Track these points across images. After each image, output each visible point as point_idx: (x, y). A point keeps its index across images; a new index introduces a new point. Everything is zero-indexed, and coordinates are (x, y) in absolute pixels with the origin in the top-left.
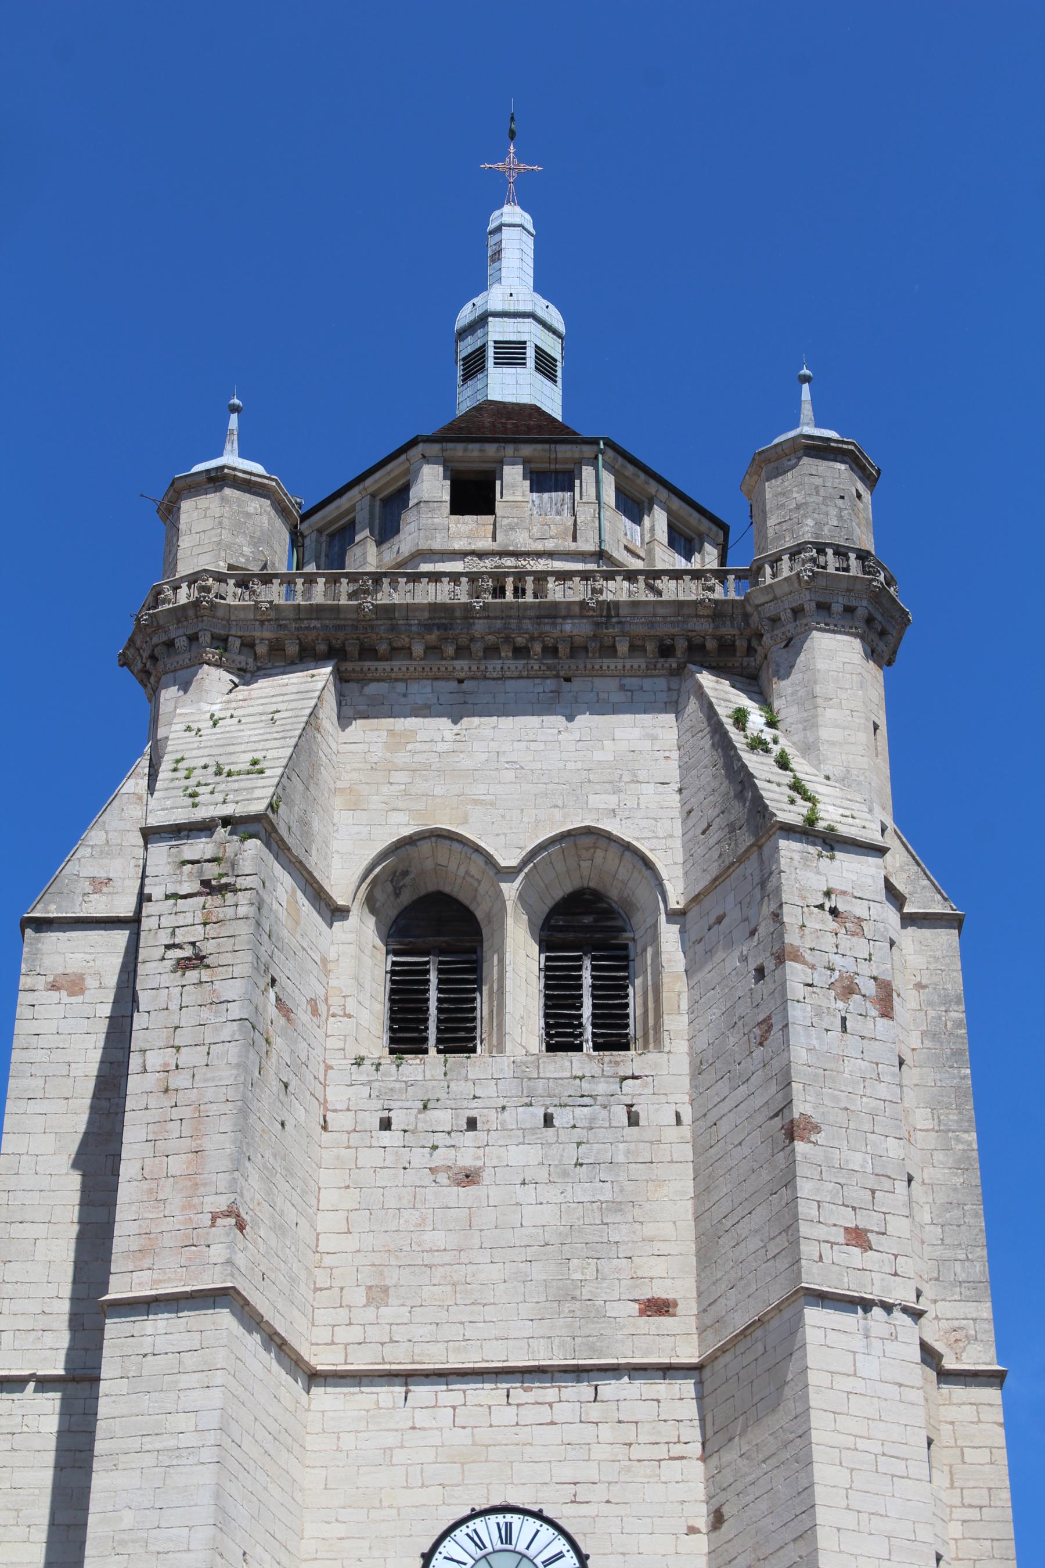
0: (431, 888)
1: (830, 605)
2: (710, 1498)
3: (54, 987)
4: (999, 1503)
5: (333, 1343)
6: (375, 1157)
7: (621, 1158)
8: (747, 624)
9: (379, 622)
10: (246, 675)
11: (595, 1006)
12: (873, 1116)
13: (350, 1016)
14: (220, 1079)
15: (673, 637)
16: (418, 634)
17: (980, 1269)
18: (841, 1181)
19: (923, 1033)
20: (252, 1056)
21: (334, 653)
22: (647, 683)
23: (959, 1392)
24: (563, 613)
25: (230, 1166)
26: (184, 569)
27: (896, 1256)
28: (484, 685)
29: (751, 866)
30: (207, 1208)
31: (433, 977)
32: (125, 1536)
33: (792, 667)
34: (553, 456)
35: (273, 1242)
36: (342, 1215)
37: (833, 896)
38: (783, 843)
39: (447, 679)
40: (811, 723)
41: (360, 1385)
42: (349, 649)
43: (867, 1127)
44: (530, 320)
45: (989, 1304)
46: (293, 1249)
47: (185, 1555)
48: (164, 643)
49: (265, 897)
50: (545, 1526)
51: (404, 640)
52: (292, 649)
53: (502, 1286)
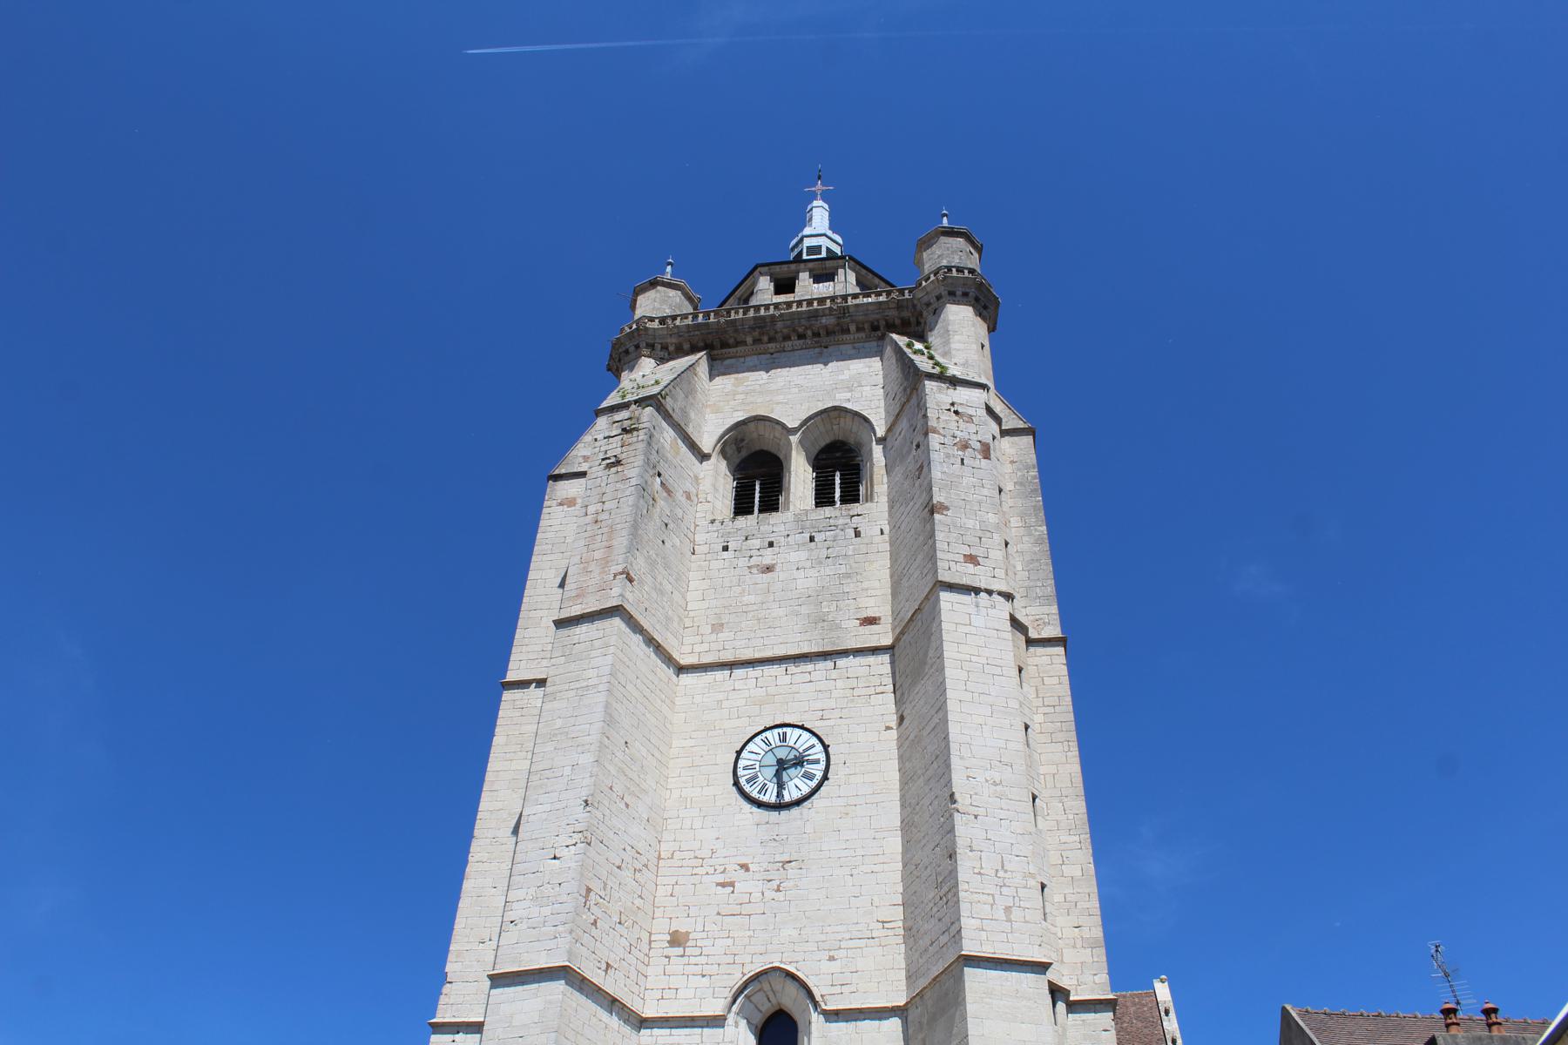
0: (758, 448)
2: (897, 711)
3: (561, 504)
5: (692, 652)
6: (720, 564)
7: (850, 553)
10: (662, 360)
11: (841, 492)
12: (980, 503)
13: (709, 502)
15: (878, 321)
16: (749, 332)
17: (1050, 589)
18: (962, 533)
19: (1015, 483)
20: (641, 501)
21: (708, 347)
22: (867, 345)
23: (1040, 650)
24: (821, 314)
26: (636, 317)
27: (994, 568)
28: (784, 354)
29: (914, 401)
32: (557, 732)
33: (937, 322)
35: (654, 595)
38: (926, 382)
39: (764, 354)
40: (947, 342)
42: (715, 343)
43: (976, 508)
44: (824, 237)
45: (1056, 606)
48: (624, 352)
50: (805, 732)
51: (741, 337)
52: (686, 346)
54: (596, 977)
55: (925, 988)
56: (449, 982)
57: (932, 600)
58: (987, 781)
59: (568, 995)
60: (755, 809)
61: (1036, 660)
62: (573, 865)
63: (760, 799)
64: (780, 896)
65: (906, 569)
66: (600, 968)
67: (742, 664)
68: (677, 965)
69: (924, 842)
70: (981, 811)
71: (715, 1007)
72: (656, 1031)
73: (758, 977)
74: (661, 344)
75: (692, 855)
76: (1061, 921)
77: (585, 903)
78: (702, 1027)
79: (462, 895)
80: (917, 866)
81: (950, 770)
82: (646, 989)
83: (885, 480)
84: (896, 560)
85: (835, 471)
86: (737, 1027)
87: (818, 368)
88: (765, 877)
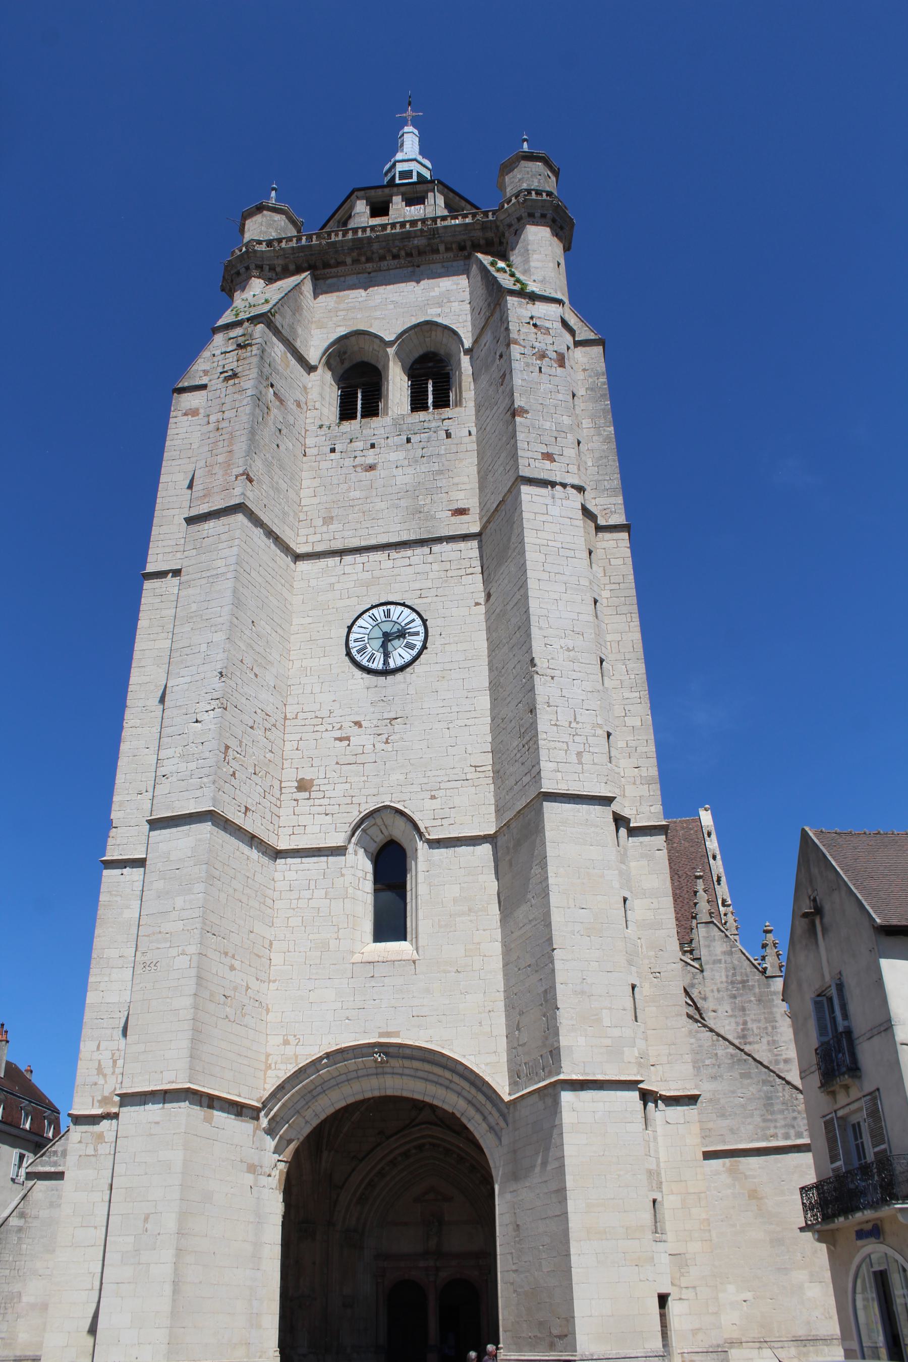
0: (359, 359)
1: (534, 214)
2: (485, 589)
3: (185, 414)
4: (628, 581)
5: (307, 542)
6: (328, 464)
7: (443, 452)
8: (498, 230)
9: (330, 250)
10: (270, 281)
11: (433, 398)
13: (317, 409)
14: (242, 421)
15: (464, 241)
17: (616, 482)
19: (587, 389)
20: (257, 409)
21: (312, 268)
22: (455, 264)
23: (607, 535)
24: (413, 235)
25: (245, 455)
27: (568, 465)
29: (497, 315)
30: (233, 474)
31: (360, 395)
32: (192, 615)
33: (518, 242)
34: (415, 190)
35: (271, 492)
36: (312, 489)
37: (534, 319)
38: (508, 298)
39: (363, 273)
40: (527, 261)
41: (319, 559)
43: (552, 412)
45: (621, 497)
46: (284, 500)
47: (218, 619)
48: (236, 273)
49: (266, 348)
50: (406, 609)
52: (292, 267)
53: (386, 511)
54: (238, 819)
55: (511, 819)
56: (115, 827)
57: (513, 493)
58: (562, 647)
59: (215, 834)
60: (365, 675)
61: (605, 544)
62: (212, 727)
63: (370, 666)
64: (389, 747)
65: (491, 466)
66: (240, 811)
67: (351, 551)
68: (304, 806)
69: (509, 699)
70: (557, 673)
71: (338, 840)
72: (289, 860)
73: (372, 814)
74: (269, 265)
75: (313, 715)
76: (623, 763)
77: (225, 758)
78: (327, 856)
79: (120, 755)
80: (503, 720)
81: (531, 638)
82: (279, 827)
83: (472, 387)
84: (483, 458)
85: (427, 380)
86: (356, 855)
87: (412, 285)
88: (375, 732)
